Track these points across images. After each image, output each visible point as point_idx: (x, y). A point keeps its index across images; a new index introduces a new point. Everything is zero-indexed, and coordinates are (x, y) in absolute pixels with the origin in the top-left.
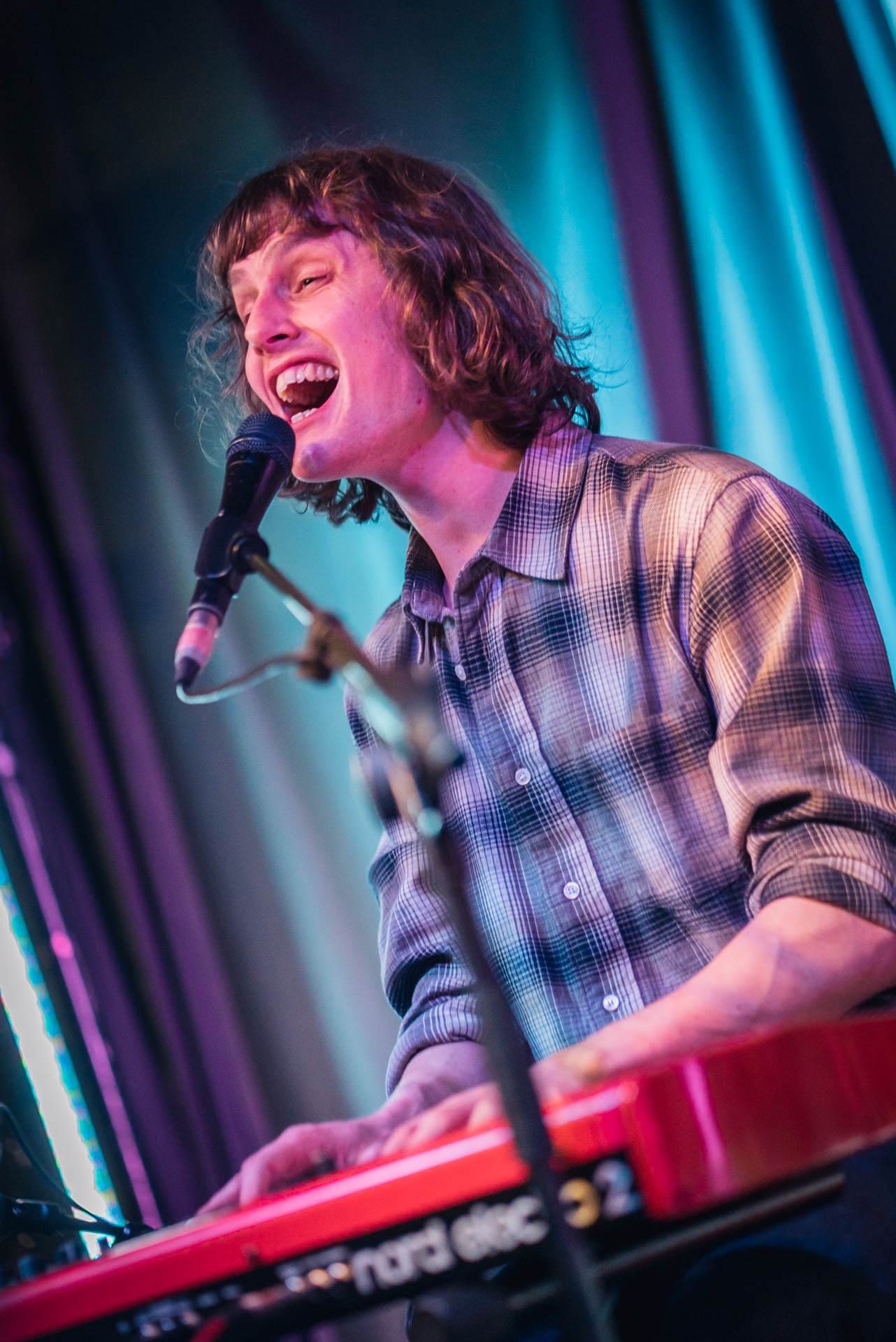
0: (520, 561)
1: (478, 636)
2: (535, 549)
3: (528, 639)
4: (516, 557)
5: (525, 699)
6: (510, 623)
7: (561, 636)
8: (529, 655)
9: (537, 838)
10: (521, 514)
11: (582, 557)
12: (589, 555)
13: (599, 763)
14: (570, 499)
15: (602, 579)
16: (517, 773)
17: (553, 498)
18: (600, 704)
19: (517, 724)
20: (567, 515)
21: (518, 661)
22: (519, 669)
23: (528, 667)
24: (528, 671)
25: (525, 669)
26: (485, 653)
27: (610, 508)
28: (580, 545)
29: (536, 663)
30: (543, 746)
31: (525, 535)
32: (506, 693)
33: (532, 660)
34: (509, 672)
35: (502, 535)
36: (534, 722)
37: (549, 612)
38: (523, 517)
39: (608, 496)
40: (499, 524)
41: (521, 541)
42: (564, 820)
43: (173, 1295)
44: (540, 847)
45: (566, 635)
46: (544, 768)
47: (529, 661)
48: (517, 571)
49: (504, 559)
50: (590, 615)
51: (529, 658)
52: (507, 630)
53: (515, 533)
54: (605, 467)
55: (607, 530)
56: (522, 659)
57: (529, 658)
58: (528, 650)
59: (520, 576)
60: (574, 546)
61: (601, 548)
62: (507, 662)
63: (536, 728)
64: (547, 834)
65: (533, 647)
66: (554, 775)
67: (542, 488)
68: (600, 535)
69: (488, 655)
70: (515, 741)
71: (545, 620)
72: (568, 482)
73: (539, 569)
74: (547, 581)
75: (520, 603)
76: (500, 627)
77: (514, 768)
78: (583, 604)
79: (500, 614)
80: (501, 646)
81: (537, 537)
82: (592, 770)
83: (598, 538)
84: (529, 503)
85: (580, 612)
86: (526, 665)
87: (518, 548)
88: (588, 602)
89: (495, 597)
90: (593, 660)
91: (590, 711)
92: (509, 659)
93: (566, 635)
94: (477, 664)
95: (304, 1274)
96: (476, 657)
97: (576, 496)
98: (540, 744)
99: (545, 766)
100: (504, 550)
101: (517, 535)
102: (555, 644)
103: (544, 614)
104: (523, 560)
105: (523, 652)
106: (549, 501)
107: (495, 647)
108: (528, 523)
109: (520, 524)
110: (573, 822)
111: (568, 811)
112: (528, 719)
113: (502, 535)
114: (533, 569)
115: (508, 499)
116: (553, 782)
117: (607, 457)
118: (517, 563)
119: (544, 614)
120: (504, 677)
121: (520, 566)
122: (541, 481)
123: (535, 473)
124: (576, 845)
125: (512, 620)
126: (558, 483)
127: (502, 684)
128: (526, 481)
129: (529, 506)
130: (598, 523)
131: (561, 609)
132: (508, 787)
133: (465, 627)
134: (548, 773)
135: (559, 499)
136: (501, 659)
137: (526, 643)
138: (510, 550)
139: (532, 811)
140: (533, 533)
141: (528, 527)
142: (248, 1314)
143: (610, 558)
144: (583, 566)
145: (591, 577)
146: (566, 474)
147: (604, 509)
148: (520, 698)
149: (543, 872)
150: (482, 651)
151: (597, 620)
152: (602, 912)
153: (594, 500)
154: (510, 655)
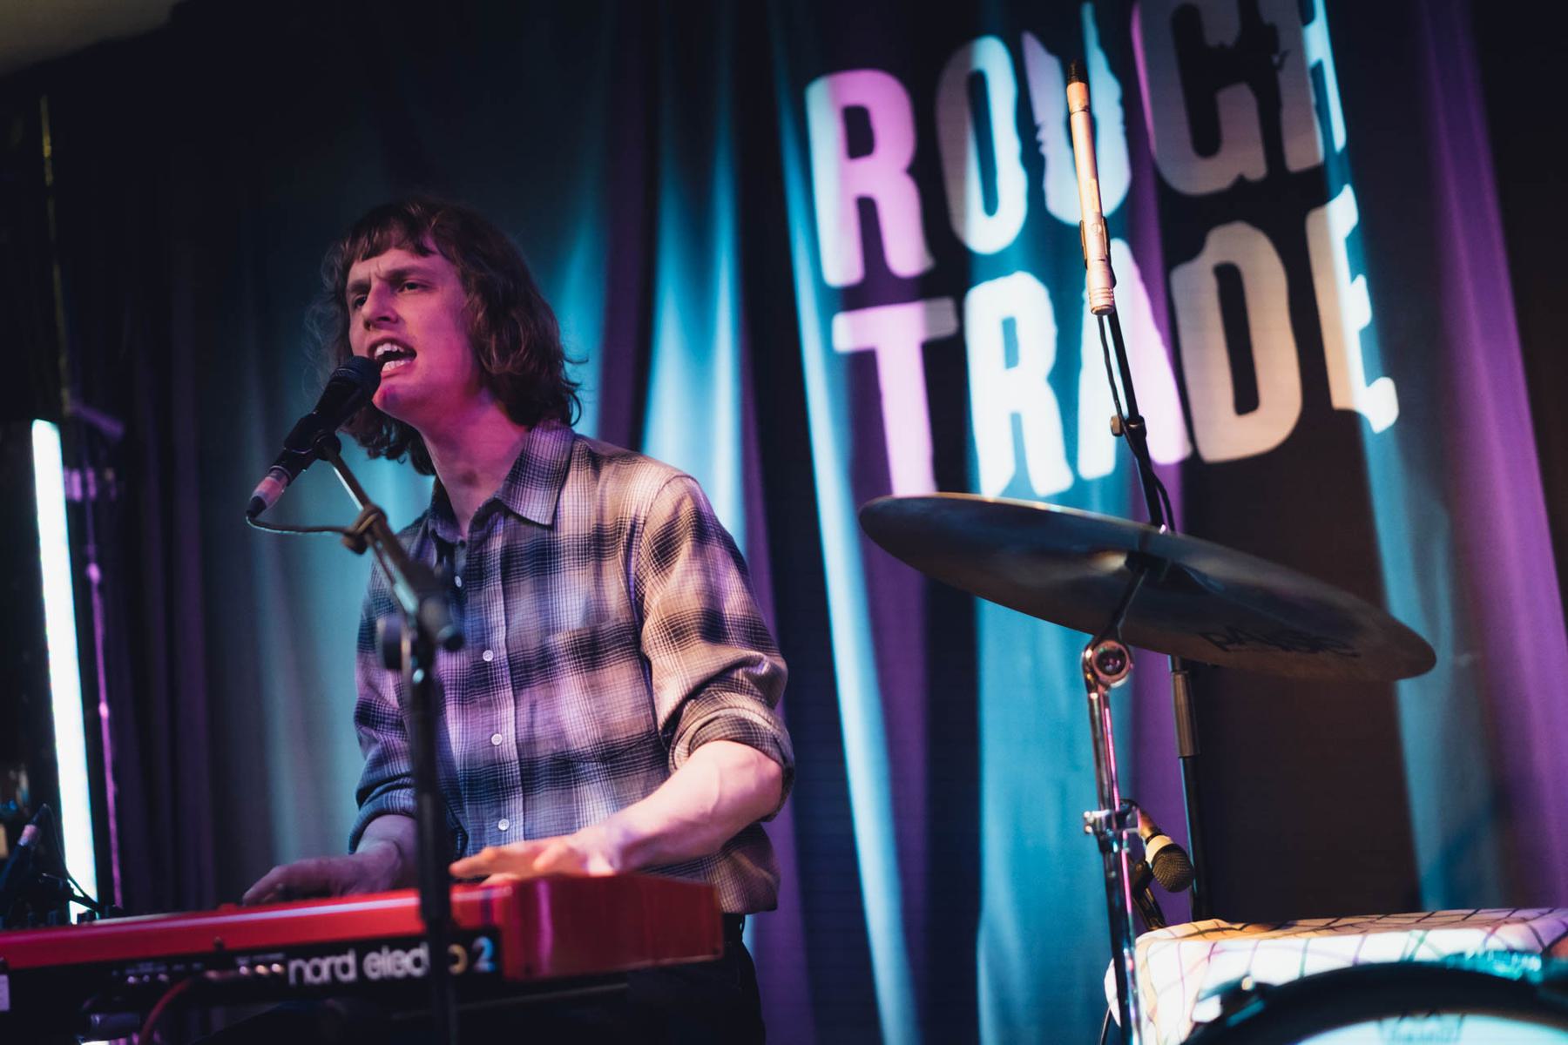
1: (481, 553)
3: (520, 563)
5: (505, 603)
7: (542, 564)
9: (485, 699)
11: (566, 512)
12: (571, 512)
13: (554, 651)
16: (484, 654)
18: (561, 614)
19: (495, 619)
24: (514, 585)
28: (566, 504)
30: (509, 637)
34: (500, 582)
36: (507, 620)
42: (506, 690)
43: (156, 960)
44: (486, 706)
45: (546, 564)
46: (504, 653)
50: (566, 553)
58: (518, 570)
60: (561, 504)
63: (507, 625)
64: (492, 697)
65: (523, 569)
66: (508, 658)
70: (490, 630)
74: (538, 525)
77: (484, 648)
78: (562, 545)
79: (501, 541)
82: (547, 656)
88: (566, 545)
90: (563, 583)
91: (553, 618)
94: (476, 572)
95: (252, 966)
96: (477, 567)
98: (506, 636)
99: (505, 652)
105: (513, 571)
110: (511, 693)
111: (510, 685)
112: (503, 617)
116: (507, 664)
120: (496, 585)
124: (509, 709)
132: (475, 659)
133: (474, 545)
134: (505, 657)
135: (551, 468)
136: (496, 572)
137: (518, 565)
139: (487, 680)
142: (210, 981)
144: (566, 519)
148: (502, 602)
149: (482, 723)
150: (481, 564)
151: (571, 557)
152: (512, 759)
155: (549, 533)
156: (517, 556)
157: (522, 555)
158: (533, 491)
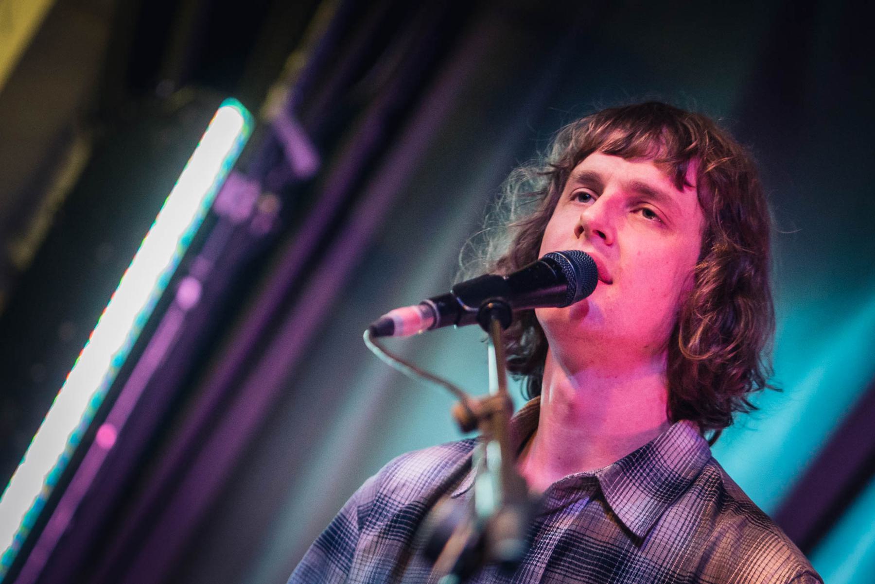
0: (617, 500)
1: (542, 523)
2: (632, 500)
4: (616, 494)
6: (572, 535)
8: (568, 567)
10: (638, 468)
11: (661, 534)
14: (678, 486)
15: (664, 561)
17: (666, 475)
20: (670, 495)
21: (556, 564)
22: (551, 569)
23: (560, 574)
25: (556, 572)
26: (536, 538)
27: (703, 515)
28: (666, 525)
29: (568, 577)
31: (631, 484)
32: (529, 577)
33: (567, 571)
34: (544, 566)
35: (617, 473)
37: (608, 552)
38: (638, 471)
39: (707, 505)
40: (620, 463)
41: (625, 488)
45: (608, 577)
47: (564, 570)
48: (611, 504)
49: (607, 490)
51: (566, 569)
52: (566, 538)
53: (626, 477)
54: (715, 483)
55: (691, 529)
56: (560, 565)
57: (566, 569)
58: (570, 563)
59: (608, 509)
61: (679, 538)
62: (548, 558)
65: (576, 565)
67: (663, 462)
68: (684, 529)
69: (537, 541)
71: (601, 555)
72: (683, 471)
73: (627, 516)
75: (591, 527)
76: (563, 531)
78: (638, 567)
80: (552, 544)
81: (638, 492)
83: (681, 530)
84: (648, 464)
85: (631, 570)
86: (559, 571)
87: (621, 490)
89: (575, 508)
92: (551, 557)
93: (608, 577)
97: (683, 487)
100: (611, 484)
101: (626, 480)
102: (595, 576)
103: (604, 551)
104: (619, 500)
105: (565, 561)
106: (662, 475)
107: (548, 541)
108: (639, 478)
109: (633, 474)
113: (617, 473)
114: (623, 512)
115: (638, 451)
117: (720, 477)
118: (614, 500)
119: (604, 551)
121: (614, 503)
122: (666, 457)
123: (666, 448)
125: (576, 534)
126: (675, 467)
127: (532, 569)
128: (657, 449)
129: (647, 467)
130: (689, 519)
131: (619, 557)
136: (546, 552)
137: (573, 558)
138: (615, 487)
140: (638, 488)
141: (636, 481)
143: (680, 550)
144: (657, 541)
145: (657, 554)
146: (684, 466)
147: (699, 513)
150: (535, 535)
153: (695, 501)
154: (554, 555)
155: (630, 546)
156: (578, 547)
157: (583, 549)
158: (634, 488)
